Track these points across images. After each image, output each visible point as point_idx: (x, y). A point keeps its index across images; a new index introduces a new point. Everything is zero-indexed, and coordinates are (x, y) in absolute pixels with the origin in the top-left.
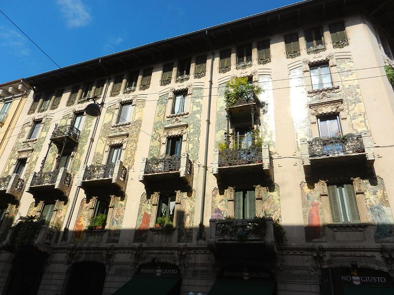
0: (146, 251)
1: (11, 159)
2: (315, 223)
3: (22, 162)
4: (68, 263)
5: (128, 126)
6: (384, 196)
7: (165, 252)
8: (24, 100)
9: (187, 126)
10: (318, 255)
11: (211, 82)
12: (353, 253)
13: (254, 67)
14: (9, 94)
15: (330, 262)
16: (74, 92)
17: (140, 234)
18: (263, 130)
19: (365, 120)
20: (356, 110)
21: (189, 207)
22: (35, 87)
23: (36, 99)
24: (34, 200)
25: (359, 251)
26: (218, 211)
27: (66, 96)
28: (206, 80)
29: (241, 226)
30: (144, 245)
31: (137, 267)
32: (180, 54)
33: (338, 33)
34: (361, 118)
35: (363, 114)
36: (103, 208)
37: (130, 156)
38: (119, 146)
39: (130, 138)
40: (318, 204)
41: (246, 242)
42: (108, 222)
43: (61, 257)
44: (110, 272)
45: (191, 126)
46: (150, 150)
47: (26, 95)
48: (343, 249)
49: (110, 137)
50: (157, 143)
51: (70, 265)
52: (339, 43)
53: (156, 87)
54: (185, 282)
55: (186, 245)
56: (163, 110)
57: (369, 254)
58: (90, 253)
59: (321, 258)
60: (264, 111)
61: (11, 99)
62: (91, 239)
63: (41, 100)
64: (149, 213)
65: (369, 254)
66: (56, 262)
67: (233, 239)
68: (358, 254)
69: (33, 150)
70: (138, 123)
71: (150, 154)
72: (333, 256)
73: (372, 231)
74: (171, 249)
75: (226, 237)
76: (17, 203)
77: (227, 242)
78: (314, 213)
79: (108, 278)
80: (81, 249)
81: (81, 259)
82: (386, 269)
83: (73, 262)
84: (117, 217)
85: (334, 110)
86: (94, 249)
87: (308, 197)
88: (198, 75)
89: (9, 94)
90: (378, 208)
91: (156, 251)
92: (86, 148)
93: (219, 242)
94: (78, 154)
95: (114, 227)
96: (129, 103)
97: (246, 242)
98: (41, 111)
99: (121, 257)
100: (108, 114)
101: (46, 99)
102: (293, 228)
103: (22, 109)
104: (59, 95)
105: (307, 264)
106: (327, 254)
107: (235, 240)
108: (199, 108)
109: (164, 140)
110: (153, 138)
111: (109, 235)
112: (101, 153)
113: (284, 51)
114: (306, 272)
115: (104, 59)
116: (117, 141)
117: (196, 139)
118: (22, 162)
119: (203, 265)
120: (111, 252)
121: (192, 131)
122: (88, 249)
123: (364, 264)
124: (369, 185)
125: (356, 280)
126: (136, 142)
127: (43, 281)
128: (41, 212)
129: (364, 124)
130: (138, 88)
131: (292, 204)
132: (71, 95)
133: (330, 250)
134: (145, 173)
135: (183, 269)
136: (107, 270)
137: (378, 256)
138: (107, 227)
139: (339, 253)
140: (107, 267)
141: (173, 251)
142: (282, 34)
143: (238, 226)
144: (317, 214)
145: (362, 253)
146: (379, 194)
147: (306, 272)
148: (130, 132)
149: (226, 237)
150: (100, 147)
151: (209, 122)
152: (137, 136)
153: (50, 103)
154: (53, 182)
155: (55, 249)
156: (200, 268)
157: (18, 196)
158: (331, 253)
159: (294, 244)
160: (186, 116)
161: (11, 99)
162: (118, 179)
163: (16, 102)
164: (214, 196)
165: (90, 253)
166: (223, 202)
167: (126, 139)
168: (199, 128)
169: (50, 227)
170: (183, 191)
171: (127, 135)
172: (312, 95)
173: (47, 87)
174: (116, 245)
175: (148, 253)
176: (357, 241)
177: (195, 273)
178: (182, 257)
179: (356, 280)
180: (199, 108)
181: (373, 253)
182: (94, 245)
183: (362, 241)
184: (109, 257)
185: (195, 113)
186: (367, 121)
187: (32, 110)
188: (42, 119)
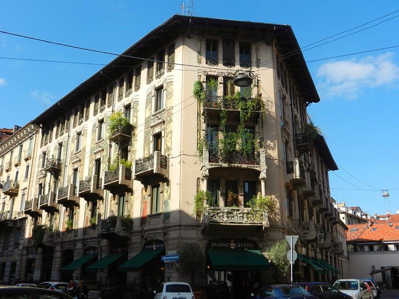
0: (87, 241)
2: (145, 215)
4: (61, 251)
7: (92, 240)
17: (85, 230)
23: (43, 135)
24: (143, 186)
27: (144, 72)
30: (86, 237)
36: (71, 216)
39: (82, 163)
42: (74, 224)
43: (58, 248)
47: (37, 132)
62: (69, 235)
63: (45, 135)
66: (57, 251)
73: (162, 217)
75: (104, 230)
80: (65, 242)
81: (65, 249)
83: (63, 250)
91: (90, 240)
95: (76, 228)
99: (79, 245)
101: (47, 134)
102: (136, 219)
111: (75, 233)
115: (61, 101)
119: (105, 246)
120: (75, 242)
122: (68, 242)
124: (166, 187)
127: (53, 263)
128: (51, 220)
131: (137, 205)
133: (147, 231)
138: (73, 228)
145: (157, 231)
146: (169, 192)
148: (81, 158)
154: (89, 188)
155: (56, 243)
160: (103, 142)
161: (31, 136)
162: (70, 197)
164: (111, 201)
173: (52, 119)
182: (69, 239)
188: (130, 103)
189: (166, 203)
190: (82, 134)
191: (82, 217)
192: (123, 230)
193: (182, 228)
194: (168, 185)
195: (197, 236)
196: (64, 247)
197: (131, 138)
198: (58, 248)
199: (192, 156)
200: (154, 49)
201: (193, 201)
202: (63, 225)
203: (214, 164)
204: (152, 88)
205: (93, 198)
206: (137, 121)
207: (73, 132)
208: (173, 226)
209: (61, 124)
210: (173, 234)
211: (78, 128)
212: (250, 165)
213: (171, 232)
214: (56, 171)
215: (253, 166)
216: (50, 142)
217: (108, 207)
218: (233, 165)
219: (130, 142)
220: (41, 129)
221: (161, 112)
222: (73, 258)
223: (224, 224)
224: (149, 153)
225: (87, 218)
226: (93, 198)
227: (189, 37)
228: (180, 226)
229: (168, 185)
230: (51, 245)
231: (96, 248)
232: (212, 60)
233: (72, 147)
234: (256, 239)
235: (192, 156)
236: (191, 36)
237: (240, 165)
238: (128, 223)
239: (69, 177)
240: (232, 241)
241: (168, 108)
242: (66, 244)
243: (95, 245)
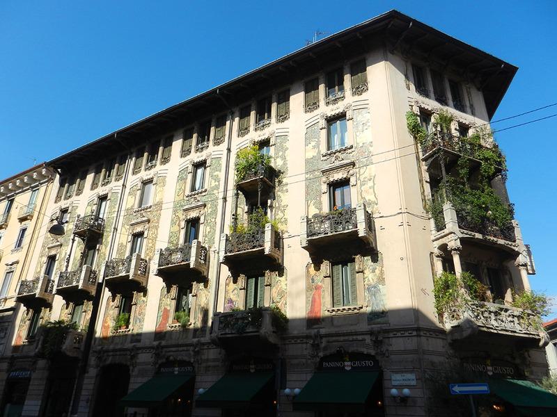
0: (165, 349)
1: (42, 256)
3: (52, 259)
5: (149, 210)
6: (382, 272)
7: (181, 349)
8: (50, 186)
9: (205, 206)
10: (377, 338)
11: (229, 150)
12: (346, 338)
13: (273, 128)
14: (35, 181)
15: (325, 348)
16: (98, 172)
18: (277, 205)
19: (374, 184)
20: (366, 175)
21: (205, 299)
22: (59, 170)
23: (62, 185)
25: (332, 336)
26: (231, 301)
28: (224, 146)
29: (241, 319)
30: (163, 343)
31: (157, 366)
32: (197, 118)
33: (359, 74)
34: (370, 183)
35: (372, 178)
36: (126, 307)
37: (151, 245)
38: (140, 235)
39: (151, 224)
40: (321, 287)
41: (245, 335)
42: (131, 320)
44: (134, 374)
45: (209, 206)
46: (170, 237)
47: (51, 180)
48: (338, 335)
49: (132, 225)
50: (176, 228)
51: (99, 368)
52: (358, 88)
53: (177, 160)
54: (198, 378)
55: (198, 341)
56: (183, 188)
57: (360, 338)
58: (116, 355)
59: (318, 345)
60: (279, 181)
61: (37, 186)
63: (67, 185)
64: (169, 308)
65: (360, 338)
67: (233, 332)
68: (351, 338)
69: (61, 245)
70: (159, 205)
71: (170, 242)
72: (328, 342)
74: (187, 345)
75: (227, 331)
76: (49, 306)
77: (228, 336)
78: (317, 297)
79: (132, 380)
80: (107, 351)
81: (108, 362)
82: (373, 352)
83: (101, 365)
84: (140, 314)
85: (345, 176)
86: (120, 350)
87: (313, 279)
88: (218, 142)
89: (35, 181)
90: (375, 287)
91: (173, 349)
92: (110, 239)
93: (223, 336)
94: (103, 246)
96: (150, 181)
97: (245, 335)
98: (67, 198)
99: (144, 357)
100: (130, 197)
101: (72, 183)
103: (46, 200)
104: (83, 178)
105: (305, 353)
106: (324, 340)
107: (232, 334)
108: (217, 183)
109: (183, 224)
110: (173, 223)
112: (125, 244)
113: (303, 103)
114: (304, 360)
115: (120, 133)
116: (138, 229)
117: (213, 220)
118: (52, 259)
119: (214, 360)
120: (135, 351)
121: (210, 210)
123: (355, 348)
125: (348, 365)
126: (157, 228)
128: (72, 314)
129: (372, 190)
130: (158, 162)
131: (297, 292)
132: (95, 177)
133: (327, 335)
134: (159, 266)
135: (197, 366)
136: (130, 372)
137: (368, 339)
139: (334, 338)
140: (131, 368)
141: (189, 348)
142: (303, 81)
143: (239, 319)
144: (320, 298)
145: (355, 337)
146: (377, 272)
147: (304, 360)
148: (151, 217)
149: (227, 331)
150: (124, 237)
151: (225, 199)
152: (158, 220)
153: (75, 187)
156: (211, 364)
157: (50, 299)
158: (327, 339)
159: (295, 333)
160: (204, 194)
161: (37, 186)
162: (135, 274)
163: (43, 188)
165: (116, 355)
166: (236, 291)
167: (147, 226)
168: (216, 206)
169: (79, 331)
170: (199, 282)
171: (149, 221)
172: (325, 158)
174: (139, 345)
175: (166, 352)
176: (352, 325)
177: (207, 368)
178: (197, 353)
179: (348, 365)
180: (217, 183)
181: (363, 337)
182: (119, 347)
183: (356, 325)
184: (133, 357)
185: (213, 189)
186: (375, 186)
187: (58, 198)
189: (373, 290)
190: (154, 183)
191: (153, 312)
192: (274, 332)
193: (422, 333)
194: (375, 260)
195: (444, 350)
196: (105, 360)
197: (274, 187)
198: (93, 360)
199: (417, 216)
200: (328, 64)
201: (430, 288)
202: (105, 321)
203: (465, 231)
204: (319, 116)
205: (181, 278)
206: (285, 164)
207: (133, 180)
208: (398, 330)
209: (103, 170)
210: (398, 344)
211: (144, 175)
212: (507, 242)
213: (394, 339)
214: (92, 236)
215: (510, 243)
216: (78, 194)
217: (221, 294)
218: (488, 237)
219: (272, 194)
220: (58, 176)
221: (345, 150)
222: (128, 382)
223: (495, 332)
224: (320, 209)
225: (166, 312)
226: (181, 278)
227: (392, 53)
228: (418, 329)
229: (375, 260)
230: (75, 355)
231: (190, 362)
232: (422, 89)
233: (131, 202)
234: (518, 361)
235: (417, 216)
236: (395, 52)
237: (495, 239)
238: (279, 320)
239: (121, 245)
240: (489, 362)
241: (361, 145)
242: (111, 353)
243: (186, 358)
